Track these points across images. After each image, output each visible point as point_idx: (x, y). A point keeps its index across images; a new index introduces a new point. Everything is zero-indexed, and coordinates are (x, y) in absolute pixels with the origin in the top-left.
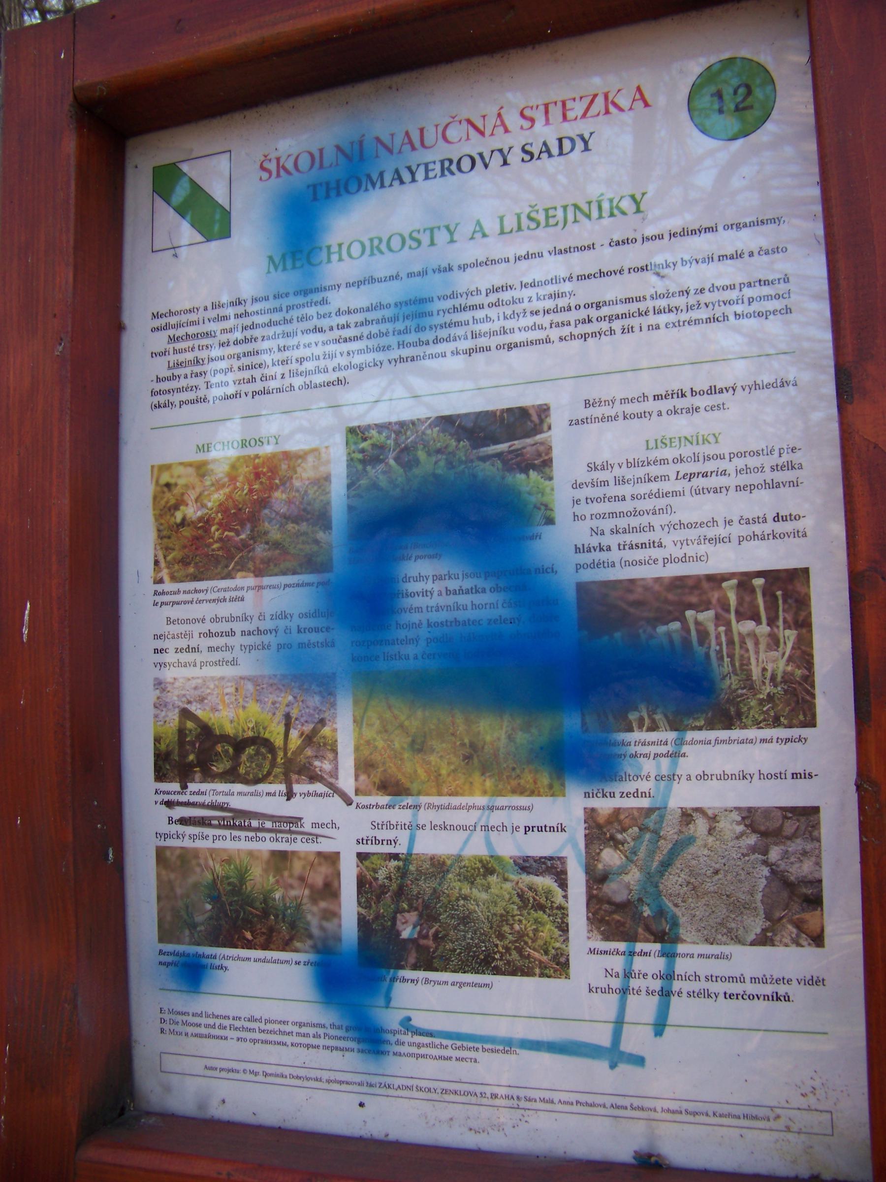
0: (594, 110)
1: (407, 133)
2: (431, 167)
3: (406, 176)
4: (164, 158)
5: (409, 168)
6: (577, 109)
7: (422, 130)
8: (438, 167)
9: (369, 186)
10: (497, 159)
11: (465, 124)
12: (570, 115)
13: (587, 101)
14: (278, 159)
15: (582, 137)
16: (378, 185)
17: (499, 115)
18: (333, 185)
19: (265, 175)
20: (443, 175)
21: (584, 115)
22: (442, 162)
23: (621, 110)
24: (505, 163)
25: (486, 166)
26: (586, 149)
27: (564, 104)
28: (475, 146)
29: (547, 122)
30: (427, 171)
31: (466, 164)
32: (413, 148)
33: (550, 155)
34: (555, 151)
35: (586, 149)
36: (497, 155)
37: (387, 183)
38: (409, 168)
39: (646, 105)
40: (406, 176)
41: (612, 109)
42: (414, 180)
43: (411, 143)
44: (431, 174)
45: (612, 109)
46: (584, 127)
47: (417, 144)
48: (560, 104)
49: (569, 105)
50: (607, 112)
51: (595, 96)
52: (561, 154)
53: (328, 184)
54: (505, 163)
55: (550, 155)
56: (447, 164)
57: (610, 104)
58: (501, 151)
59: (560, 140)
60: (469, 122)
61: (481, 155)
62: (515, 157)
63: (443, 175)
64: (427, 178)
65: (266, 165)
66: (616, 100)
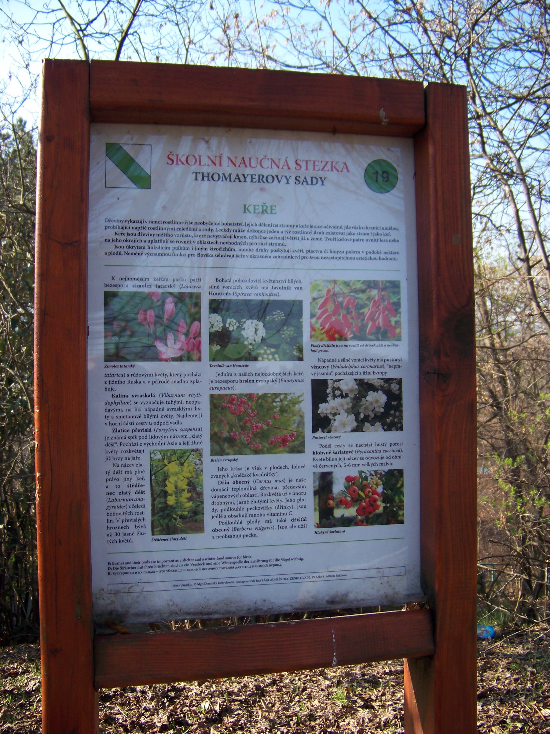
0: (325, 169)
1: (243, 159)
2: (254, 177)
3: (242, 179)
4: (114, 140)
5: (244, 175)
6: (320, 166)
7: (250, 159)
8: (257, 177)
9: (224, 179)
10: (284, 180)
11: (270, 160)
12: (317, 168)
13: (324, 163)
14: (177, 156)
15: (321, 178)
16: (228, 179)
17: (286, 161)
18: (206, 174)
19: (170, 162)
20: (259, 182)
21: (323, 169)
22: (259, 176)
23: (338, 171)
24: (288, 183)
25: (279, 182)
26: (323, 184)
27: (314, 162)
28: (275, 171)
29: (307, 169)
30: (252, 178)
31: (270, 179)
32: (246, 166)
33: (307, 184)
34: (310, 182)
35: (323, 184)
36: (284, 178)
37: (233, 179)
38: (244, 175)
39: (348, 171)
40: (242, 179)
41: (334, 169)
42: (245, 181)
43: (244, 163)
44: (254, 180)
45: (334, 169)
46: (321, 174)
47: (248, 164)
48: (312, 162)
49: (317, 163)
50: (332, 170)
51: (327, 163)
52: (312, 184)
53: (203, 173)
54: (288, 183)
55: (307, 184)
56: (261, 177)
57: (333, 168)
58: (286, 177)
59: (312, 178)
60: (272, 159)
61: (277, 176)
62: (292, 181)
63: (259, 182)
64: (252, 181)
65: (171, 157)
66: (336, 166)
